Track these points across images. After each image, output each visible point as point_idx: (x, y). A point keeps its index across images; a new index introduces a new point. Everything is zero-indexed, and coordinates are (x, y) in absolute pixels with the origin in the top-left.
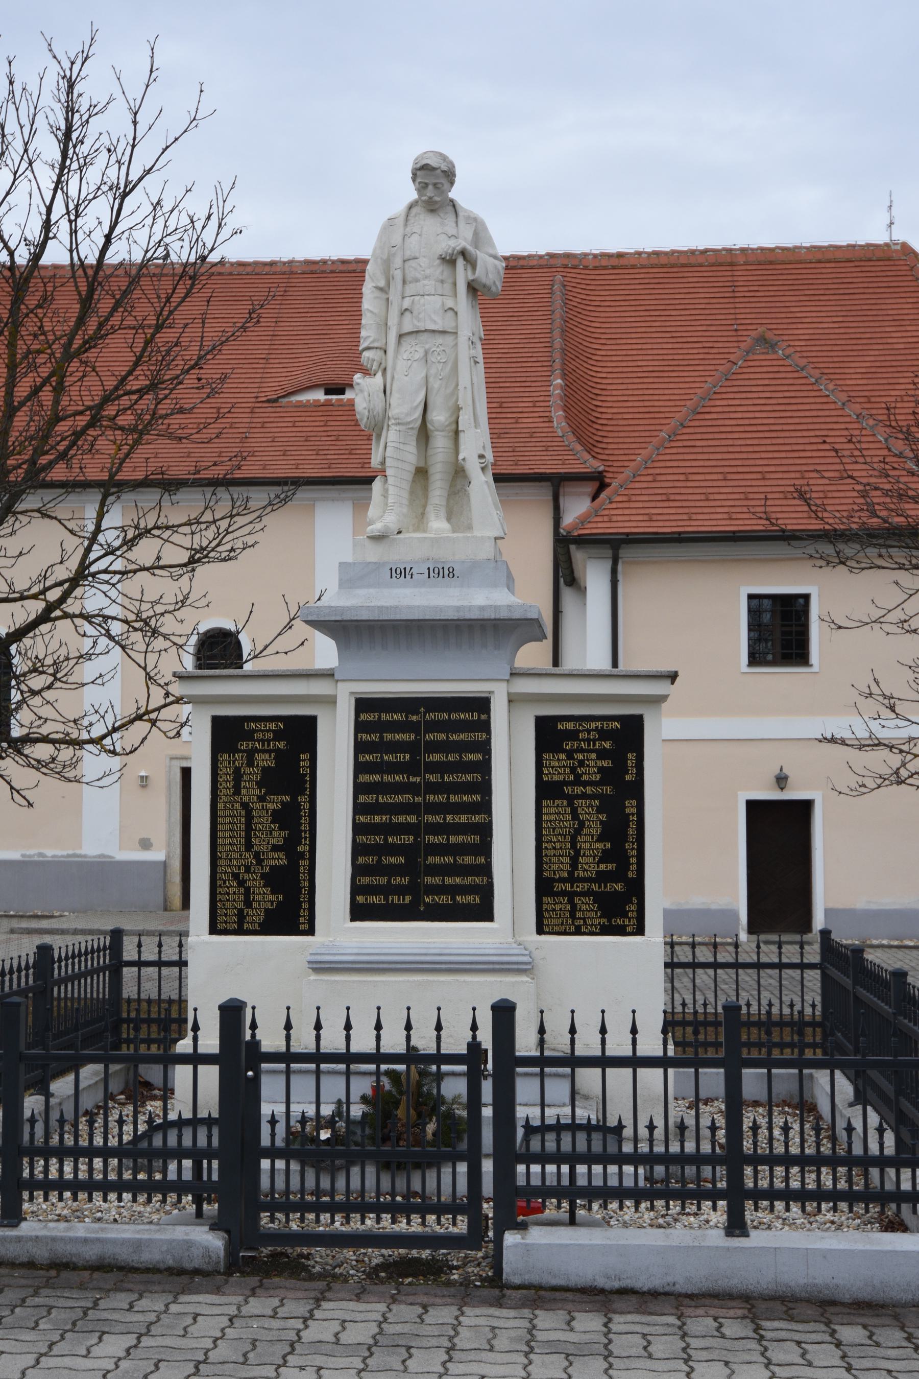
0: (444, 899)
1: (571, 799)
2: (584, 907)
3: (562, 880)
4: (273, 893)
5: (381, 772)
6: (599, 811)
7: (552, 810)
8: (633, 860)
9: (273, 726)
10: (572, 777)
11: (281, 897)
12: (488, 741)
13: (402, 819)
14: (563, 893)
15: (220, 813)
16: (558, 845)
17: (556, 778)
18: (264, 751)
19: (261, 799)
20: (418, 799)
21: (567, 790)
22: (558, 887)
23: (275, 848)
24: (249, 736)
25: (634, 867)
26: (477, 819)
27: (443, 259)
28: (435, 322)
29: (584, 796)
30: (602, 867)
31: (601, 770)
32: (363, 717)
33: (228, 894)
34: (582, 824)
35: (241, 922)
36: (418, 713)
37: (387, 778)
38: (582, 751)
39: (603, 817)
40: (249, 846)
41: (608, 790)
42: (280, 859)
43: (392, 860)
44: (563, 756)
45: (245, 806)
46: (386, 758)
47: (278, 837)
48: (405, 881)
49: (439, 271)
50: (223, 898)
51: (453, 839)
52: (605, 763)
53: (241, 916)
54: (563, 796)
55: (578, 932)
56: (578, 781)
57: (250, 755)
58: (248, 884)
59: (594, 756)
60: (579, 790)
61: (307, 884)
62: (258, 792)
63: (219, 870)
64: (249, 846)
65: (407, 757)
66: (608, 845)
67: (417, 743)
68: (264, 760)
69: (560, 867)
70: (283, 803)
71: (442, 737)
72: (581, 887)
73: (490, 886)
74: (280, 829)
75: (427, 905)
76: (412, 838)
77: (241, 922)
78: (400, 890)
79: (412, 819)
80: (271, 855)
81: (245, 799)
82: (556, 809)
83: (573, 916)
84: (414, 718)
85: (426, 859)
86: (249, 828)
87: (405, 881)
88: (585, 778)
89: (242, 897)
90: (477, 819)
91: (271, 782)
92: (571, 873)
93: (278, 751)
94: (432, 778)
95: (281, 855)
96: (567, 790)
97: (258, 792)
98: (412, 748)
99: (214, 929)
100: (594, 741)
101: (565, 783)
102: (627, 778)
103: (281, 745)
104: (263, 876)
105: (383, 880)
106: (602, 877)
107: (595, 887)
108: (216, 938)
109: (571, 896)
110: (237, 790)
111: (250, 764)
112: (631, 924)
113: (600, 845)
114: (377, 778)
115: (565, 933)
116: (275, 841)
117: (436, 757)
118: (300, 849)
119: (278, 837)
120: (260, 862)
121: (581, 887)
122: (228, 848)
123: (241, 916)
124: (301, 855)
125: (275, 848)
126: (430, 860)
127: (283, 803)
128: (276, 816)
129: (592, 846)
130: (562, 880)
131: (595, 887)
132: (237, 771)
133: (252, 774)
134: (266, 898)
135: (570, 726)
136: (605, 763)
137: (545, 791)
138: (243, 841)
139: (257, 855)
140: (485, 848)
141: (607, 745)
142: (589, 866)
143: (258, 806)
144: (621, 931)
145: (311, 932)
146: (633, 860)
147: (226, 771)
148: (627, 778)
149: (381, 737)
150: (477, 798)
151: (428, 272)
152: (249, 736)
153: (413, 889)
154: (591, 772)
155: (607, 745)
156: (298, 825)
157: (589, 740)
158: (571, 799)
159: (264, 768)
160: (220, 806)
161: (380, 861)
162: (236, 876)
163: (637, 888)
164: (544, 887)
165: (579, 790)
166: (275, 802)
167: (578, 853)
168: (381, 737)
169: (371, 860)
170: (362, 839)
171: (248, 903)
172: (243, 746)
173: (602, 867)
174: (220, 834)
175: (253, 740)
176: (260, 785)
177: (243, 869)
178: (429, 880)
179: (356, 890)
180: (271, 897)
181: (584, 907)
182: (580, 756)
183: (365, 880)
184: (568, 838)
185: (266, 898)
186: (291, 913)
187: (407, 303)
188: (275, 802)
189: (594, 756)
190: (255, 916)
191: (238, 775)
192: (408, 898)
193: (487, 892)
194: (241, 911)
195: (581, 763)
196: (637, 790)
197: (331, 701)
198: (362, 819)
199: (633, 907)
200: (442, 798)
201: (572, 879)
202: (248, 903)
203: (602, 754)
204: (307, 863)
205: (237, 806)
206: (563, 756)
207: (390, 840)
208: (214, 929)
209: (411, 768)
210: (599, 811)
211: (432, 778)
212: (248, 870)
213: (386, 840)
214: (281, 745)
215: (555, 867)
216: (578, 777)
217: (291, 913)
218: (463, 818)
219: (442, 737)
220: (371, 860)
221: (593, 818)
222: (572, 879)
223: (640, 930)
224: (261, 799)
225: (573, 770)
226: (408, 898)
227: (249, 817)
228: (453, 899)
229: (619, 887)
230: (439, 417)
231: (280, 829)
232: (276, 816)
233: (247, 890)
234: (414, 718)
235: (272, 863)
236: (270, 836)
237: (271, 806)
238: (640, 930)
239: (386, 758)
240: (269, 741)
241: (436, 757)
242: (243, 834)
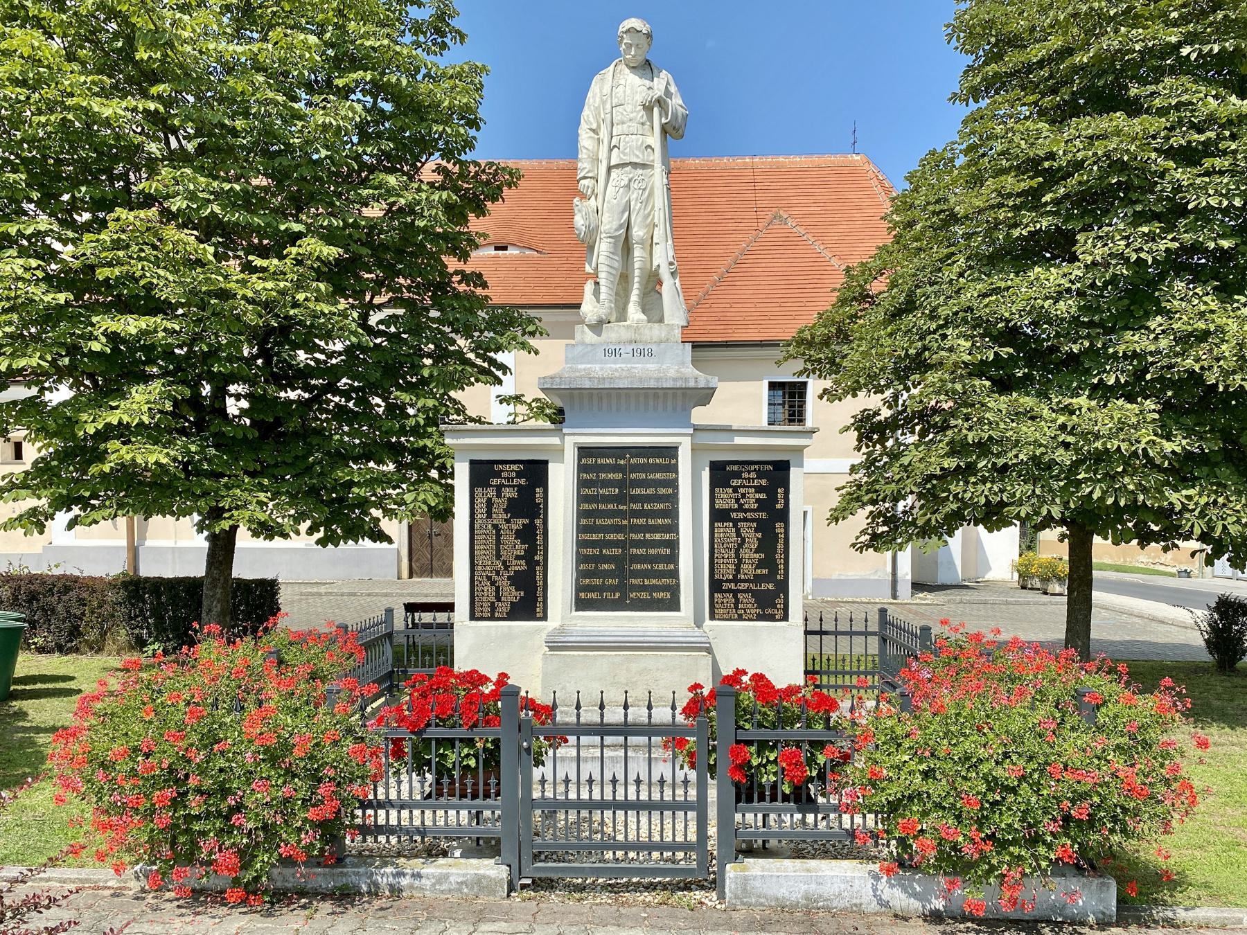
0: (644, 595)
1: (735, 522)
3: (728, 581)
5: (598, 502)
6: (756, 531)
9: (515, 467)
10: (736, 506)
12: (677, 480)
13: (613, 536)
14: (729, 591)
17: (724, 507)
20: (625, 522)
21: (733, 515)
22: (726, 586)
23: (518, 558)
24: (498, 475)
26: (668, 537)
29: (745, 520)
30: (758, 572)
31: (758, 501)
34: (743, 540)
37: (602, 507)
38: (744, 487)
39: (759, 535)
40: (498, 556)
41: (764, 515)
42: (521, 566)
43: (606, 567)
44: (730, 490)
45: (495, 526)
47: (521, 549)
48: (615, 582)
51: (650, 551)
52: (762, 496)
54: (730, 520)
55: (740, 618)
56: (741, 509)
57: (499, 488)
60: (741, 515)
64: (498, 556)
67: (624, 480)
68: (510, 493)
69: (726, 571)
71: (642, 476)
72: (742, 586)
73: (678, 585)
78: (612, 589)
79: (621, 537)
80: (515, 562)
81: (496, 522)
82: (725, 529)
83: (736, 608)
84: (622, 462)
87: (615, 582)
88: (746, 507)
90: (668, 537)
91: (514, 509)
94: (634, 506)
95: (523, 562)
96: (733, 515)
98: (621, 484)
99: (473, 617)
102: (778, 506)
103: (523, 482)
104: (509, 578)
105: (599, 582)
106: (758, 579)
107: (753, 586)
108: (474, 623)
109: (735, 592)
110: (489, 515)
113: (757, 556)
114: (594, 506)
115: (730, 619)
117: (637, 491)
119: (521, 549)
121: (742, 586)
123: (493, 606)
124: (538, 563)
125: (518, 558)
128: (519, 534)
129: (751, 556)
131: (753, 586)
132: (489, 500)
134: (512, 595)
135: (735, 468)
136: (762, 496)
137: (718, 516)
139: (504, 563)
140: (673, 558)
141: (764, 482)
142: (748, 570)
144: (771, 618)
145: (545, 618)
147: (481, 501)
148: (778, 506)
150: (668, 521)
153: (622, 587)
155: (764, 482)
156: (533, 538)
158: (735, 522)
161: (596, 567)
162: (489, 578)
163: (783, 587)
164: (716, 586)
165: (741, 515)
167: (740, 561)
169: (591, 567)
171: (498, 598)
172: (494, 482)
173: (758, 572)
175: (500, 477)
178: (633, 581)
179: (579, 589)
180: (515, 593)
182: (743, 491)
185: (512, 595)
186: (528, 603)
187: (614, 142)
190: (503, 607)
191: (490, 503)
192: (618, 595)
193: (675, 590)
195: (744, 496)
196: (784, 516)
197: (560, 451)
198: (584, 537)
200: (642, 521)
201: (735, 580)
202: (498, 598)
203: (759, 489)
205: (490, 527)
206: (730, 490)
208: (473, 617)
209: (619, 499)
210: (756, 531)
211: (634, 506)
212: (498, 573)
214: (523, 482)
215: (723, 572)
216: (741, 505)
217: (528, 603)
218: (658, 536)
219: (642, 476)
220: (591, 567)
222: (735, 580)
223: (785, 618)
224: (508, 521)
225: (737, 501)
227: (498, 535)
228: (651, 595)
229: (771, 586)
230: (637, 232)
232: (519, 534)
234: (622, 462)
235: (517, 568)
241: (637, 491)
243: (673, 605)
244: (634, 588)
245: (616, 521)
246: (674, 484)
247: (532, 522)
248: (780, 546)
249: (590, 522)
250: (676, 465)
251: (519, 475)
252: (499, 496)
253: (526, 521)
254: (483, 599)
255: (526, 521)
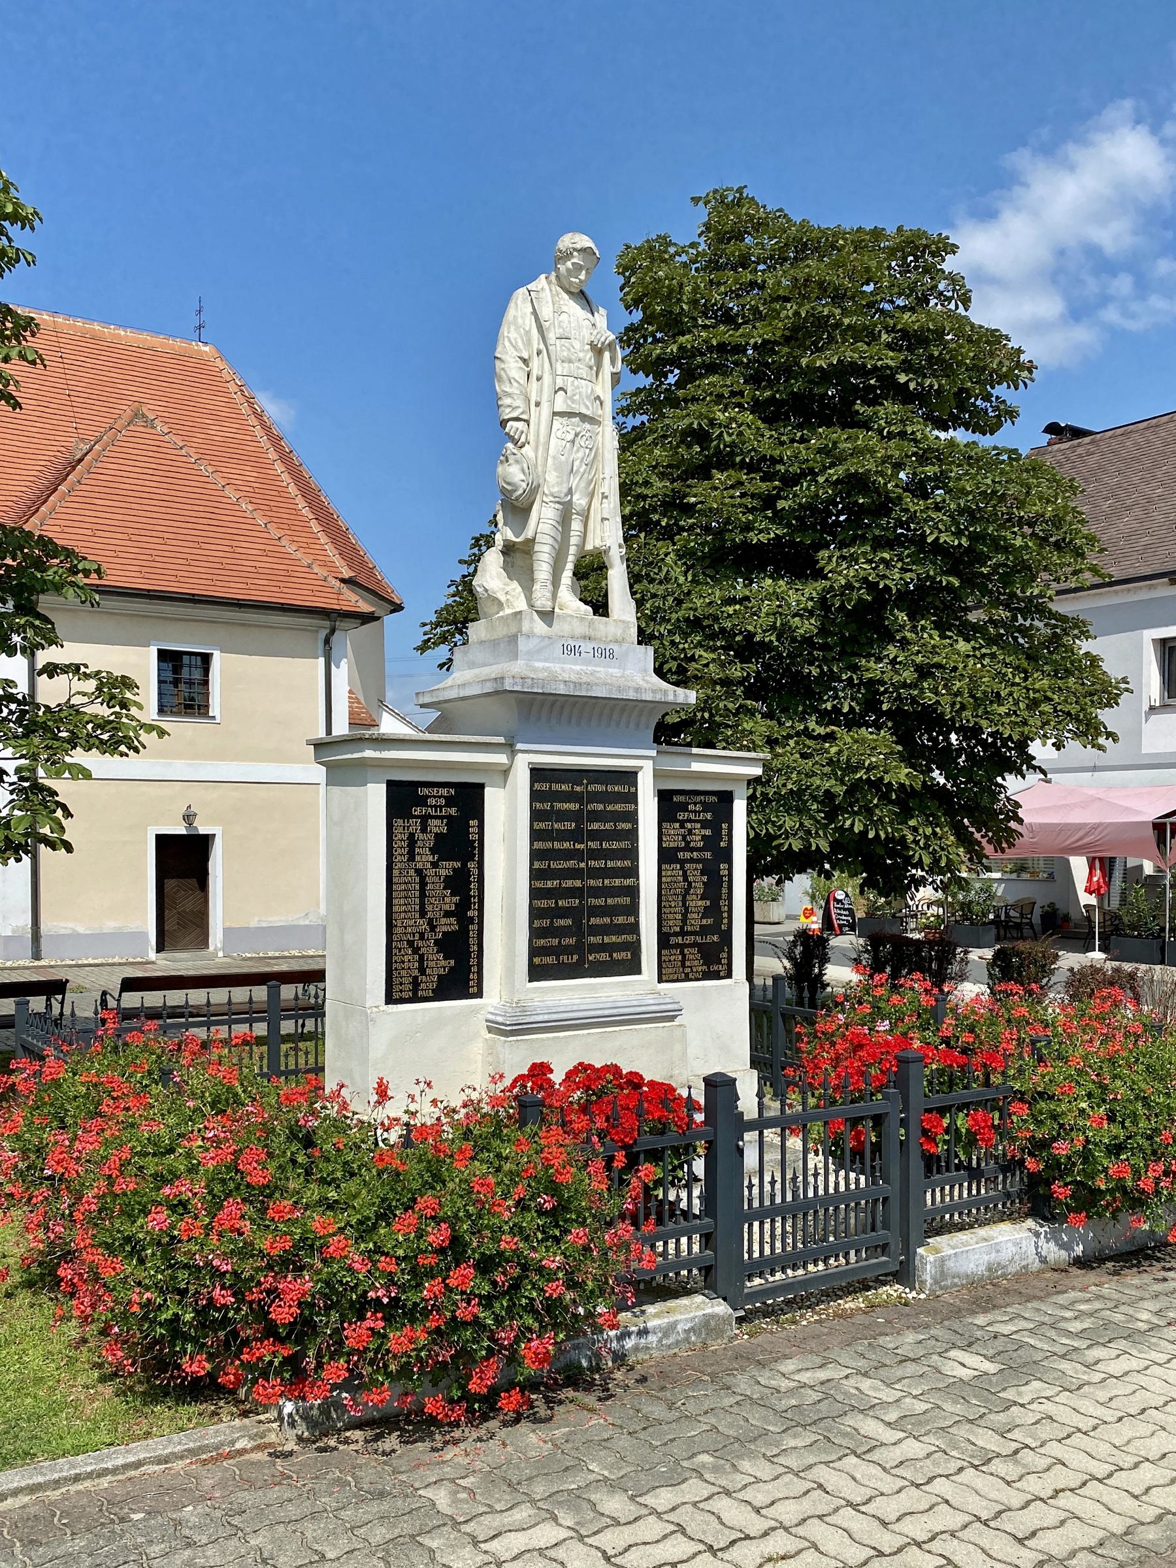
1: (682, 862)
2: (691, 957)
3: (676, 934)
4: (445, 958)
6: (702, 874)
7: (669, 873)
8: (725, 915)
10: (683, 844)
11: (452, 962)
13: (569, 883)
14: (677, 946)
15: (395, 880)
16: (673, 904)
17: (672, 845)
18: (436, 817)
19: (435, 865)
20: (583, 865)
21: (680, 855)
23: (448, 914)
24: (422, 801)
25: (725, 921)
27: (592, 345)
28: (587, 407)
29: (692, 860)
30: (704, 922)
31: (704, 837)
32: (537, 786)
33: (403, 962)
35: (415, 990)
36: (581, 784)
37: (557, 845)
38: (690, 821)
39: (705, 879)
40: (423, 913)
42: (449, 925)
44: (677, 825)
45: (419, 872)
46: (556, 826)
47: (451, 902)
48: (572, 941)
49: (589, 356)
50: (398, 966)
52: (708, 832)
53: (416, 983)
54: (678, 861)
55: (687, 979)
56: (688, 848)
57: (425, 819)
58: (422, 951)
59: (698, 825)
60: (688, 855)
61: (476, 948)
62: (431, 858)
63: (395, 938)
64: (423, 913)
65: (574, 825)
66: (708, 903)
68: (437, 826)
70: (454, 870)
72: (689, 939)
73: (639, 941)
74: (452, 895)
75: (590, 962)
76: (577, 901)
77: (415, 990)
78: (568, 951)
80: (443, 921)
83: (683, 966)
84: (578, 789)
85: (589, 921)
86: (423, 895)
87: (572, 941)
88: (692, 844)
89: (416, 964)
92: (682, 928)
93: (449, 817)
95: (453, 920)
96: (680, 855)
97: (431, 858)
98: (577, 816)
99: (390, 999)
100: (699, 812)
101: (678, 849)
102: (722, 844)
103: (453, 811)
104: (437, 942)
105: (555, 942)
106: (704, 930)
108: (393, 1008)
109: (682, 947)
110: (412, 857)
111: (424, 830)
112: (722, 969)
114: (549, 845)
115: (678, 980)
116: (447, 907)
117: (595, 826)
118: (470, 914)
119: (451, 902)
120: (433, 928)
121: (689, 939)
122: (403, 915)
123: (416, 983)
124: (471, 920)
125: (448, 914)
126: (593, 921)
127: (454, 870)
128: (449, 882)
129: (697, 904)
130: (676, 934)
132: (411, 835)
133: (426, 841)
134: (439, 964)
135: (682, 798)
136: (708, 832)
138: (417, 907)
140: (633, 909)
141: (709, 816)
143: (432, 872)
144: (716, 976)
145: (479, 994)
146: (725, 915)
147: (400, 836)
148: (722, 844)
149: (552, 806)
151: (581, 355)
152: (422, 801)
153: (579, 948)
154: (697, 841)
155: (709, 816)
156: (466, 889)
157: (695, 811)
159: (436, 834)
160: (396, 872)
162: (410, 943)
165: (688, 855)
166: (447, 868)
167: (687, 909)
168: (552, 806)
169: (546, 923)
170: (539, 903)
171: (422, 970)
172: (417, 811)
173: (704, 922)
174: (395, 901)
176: (433, 851)
177: (417, 937)
179: (533, 952)
180: (443, 963)
181: (691, 957)
182: (689, 825)
183: (542, 942)
184: (680, 898)
185: (439, 964)
186: (460, 977)
187: (560, 382)
188: (447, 868)
189: (698, 825)
190: (428, 984)
191: (412, 841)
192: (575, 957)
193: (635, 948)
194: (415, 978)
195: (690, 832)
197: (505, 772)
199: (725, 955)
200: (601, 864)
202: (422, 970)
203: (705, 824)
204: (476, 927)
205: (412, 872)
206: (677, 825)
207: (560, 903)
208: (390, 999)
210: (702, 874)
212: (422, 937)
213: (557, 903)
214: (453, 811)
215: (671, 923)
217: (460, 977)
218: (617, 882)
220: (546, 923)
221: (699, 881)
222: (683, 933)
223: (729, 975)
225: (684, 837)
226: (575, 957)
227: (423, 884)
229: (715, 938)
231: (452, 895)
232: (449, 882)
233: (422, 957)
234: (578, 789)
235: (445, 929)
236: (443, 901)
237: (443, 872)
238: (729, 975)
239: (556, 826)
240: (441, 807)
241: (595, 826)
242: (417, 901)
243: (634, 967)
244: (595, 948)
245: (571, 864)
246: (632, 817)
247: (464, 865)
248: (724, 891)
249: (543, 865)
250: (635, 794)
251: (450, 802)
252: (424, 830)
253: (458, 865)
254: (404, 973)
255: (458, 865)
